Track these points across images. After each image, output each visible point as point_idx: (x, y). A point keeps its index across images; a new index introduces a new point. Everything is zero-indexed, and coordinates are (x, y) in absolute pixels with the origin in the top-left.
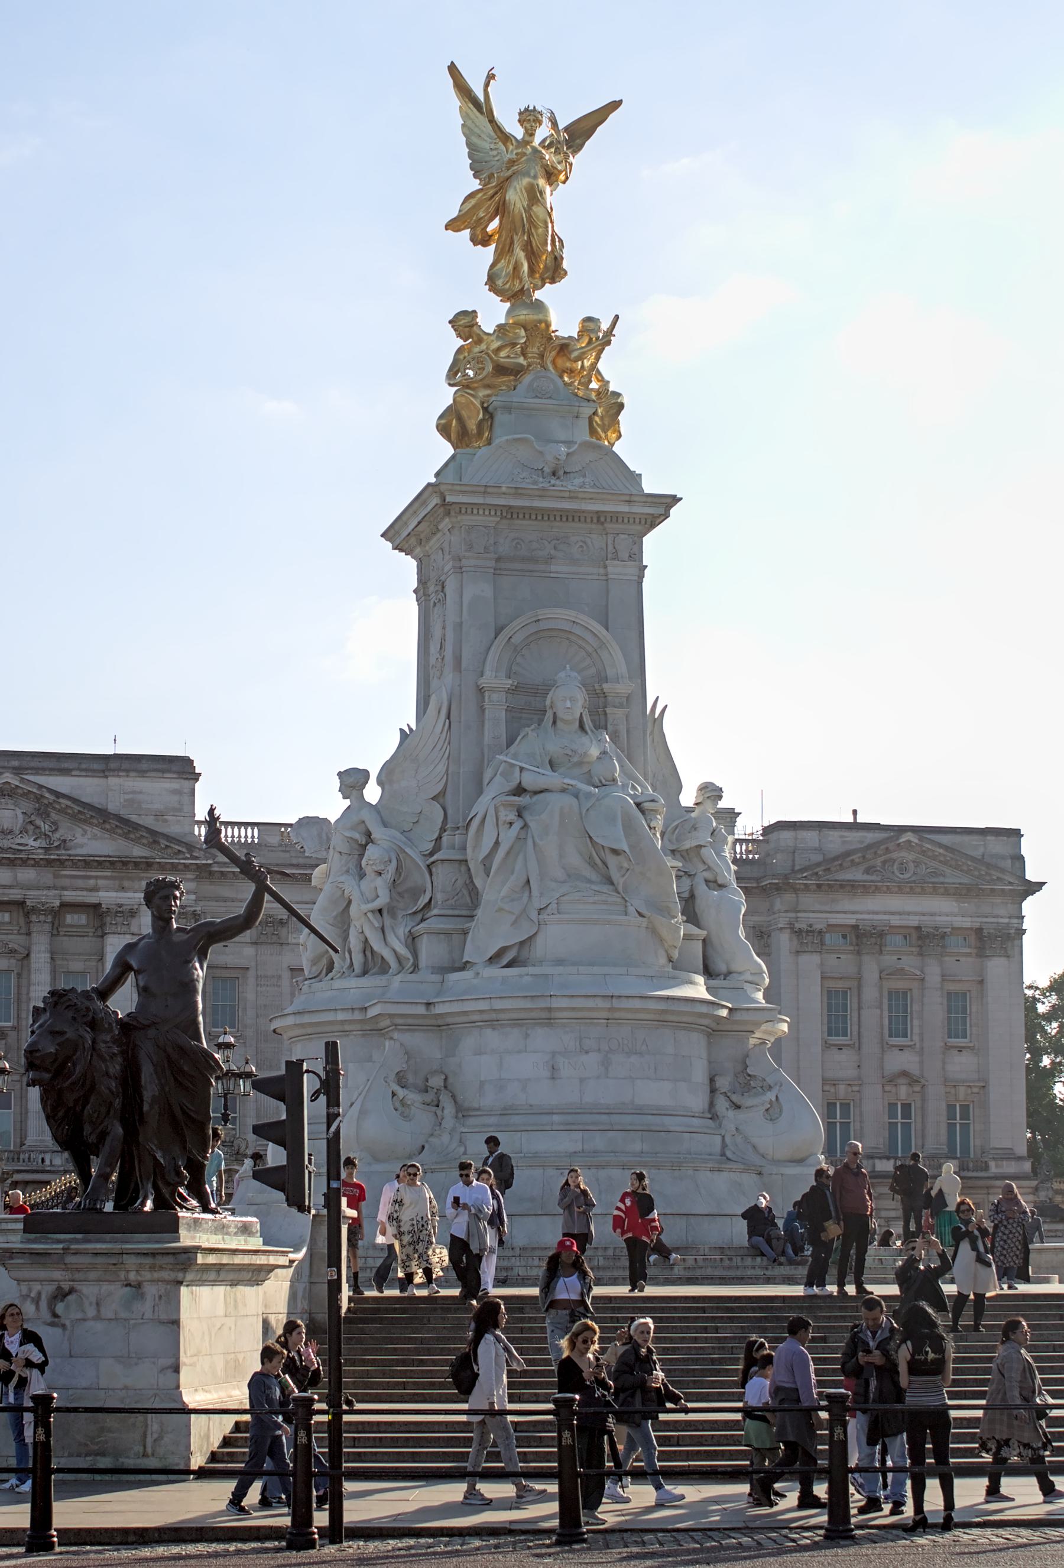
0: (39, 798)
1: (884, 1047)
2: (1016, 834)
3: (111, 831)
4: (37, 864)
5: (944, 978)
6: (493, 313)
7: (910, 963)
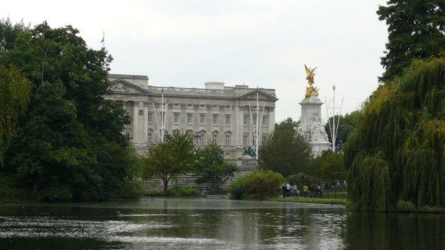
2: (274, 90)
6: (309, 86)
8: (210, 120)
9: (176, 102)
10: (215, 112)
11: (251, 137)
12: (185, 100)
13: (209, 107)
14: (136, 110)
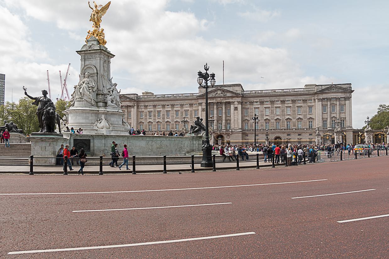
1: (331, 113)
3: (231, 93)
4: (223, 97)
7: (335, 102)
8: (295, 111)
9: (266, 100)
12: (274, 98)
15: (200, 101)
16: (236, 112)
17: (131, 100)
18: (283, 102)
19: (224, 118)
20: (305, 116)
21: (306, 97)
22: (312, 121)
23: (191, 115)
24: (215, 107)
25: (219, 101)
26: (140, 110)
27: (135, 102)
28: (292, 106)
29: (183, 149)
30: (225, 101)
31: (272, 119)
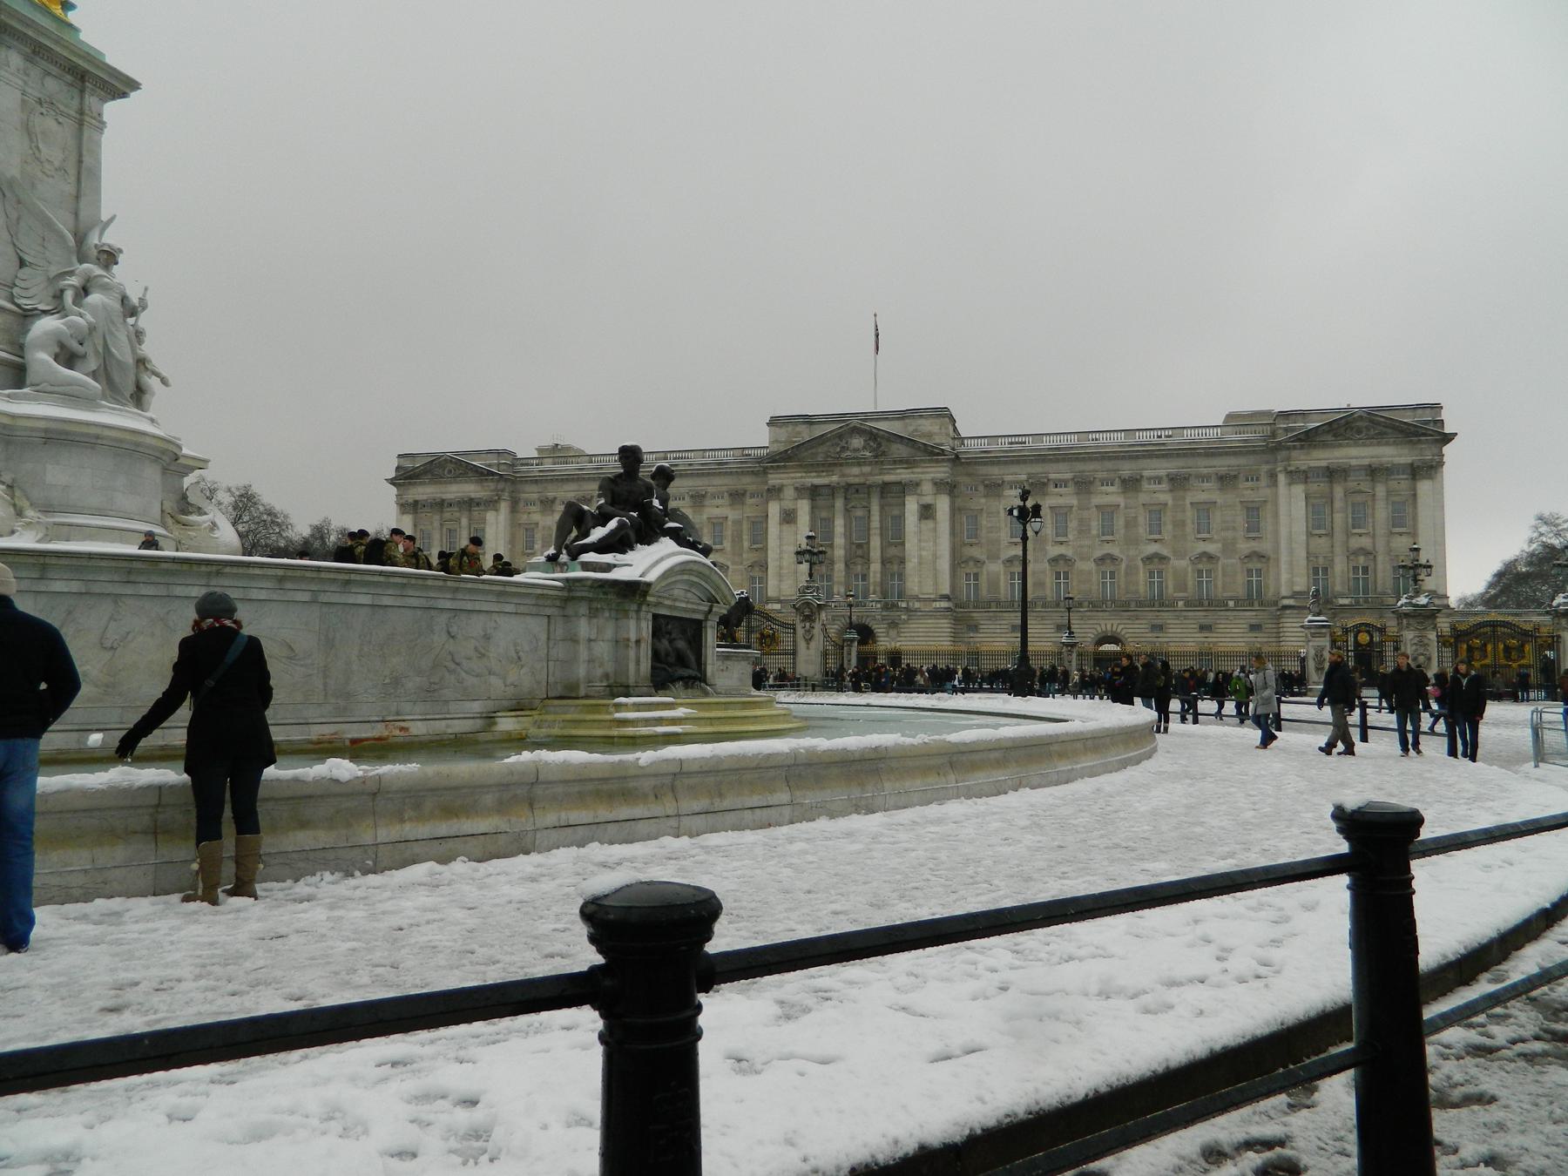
0: (871, 433)
1: (1348, 535)
2: (1436, 407)
4: (870, 464)
5: (1389, 493)
7: (1365, 486)
8: (1183, 524)
10: (1203, 497)
11: (1340, 567)
13: (1178, 482)
14: (912, 506)
15: (774, 479)
16: (929, 524)
17: (482, 475)
18: (1131, 484)
19: (875, 554)
20: (1229, 548)
21: (1233, 461)
22: (1259, 572)
23: (737, 539)
24: (839, 503)
25: (857, 480)
26: (524, 518)
27: (501, 485)
28: (1170, 502)
29: (470, 681)
30: (879, 479)
31: (1082, 559)
